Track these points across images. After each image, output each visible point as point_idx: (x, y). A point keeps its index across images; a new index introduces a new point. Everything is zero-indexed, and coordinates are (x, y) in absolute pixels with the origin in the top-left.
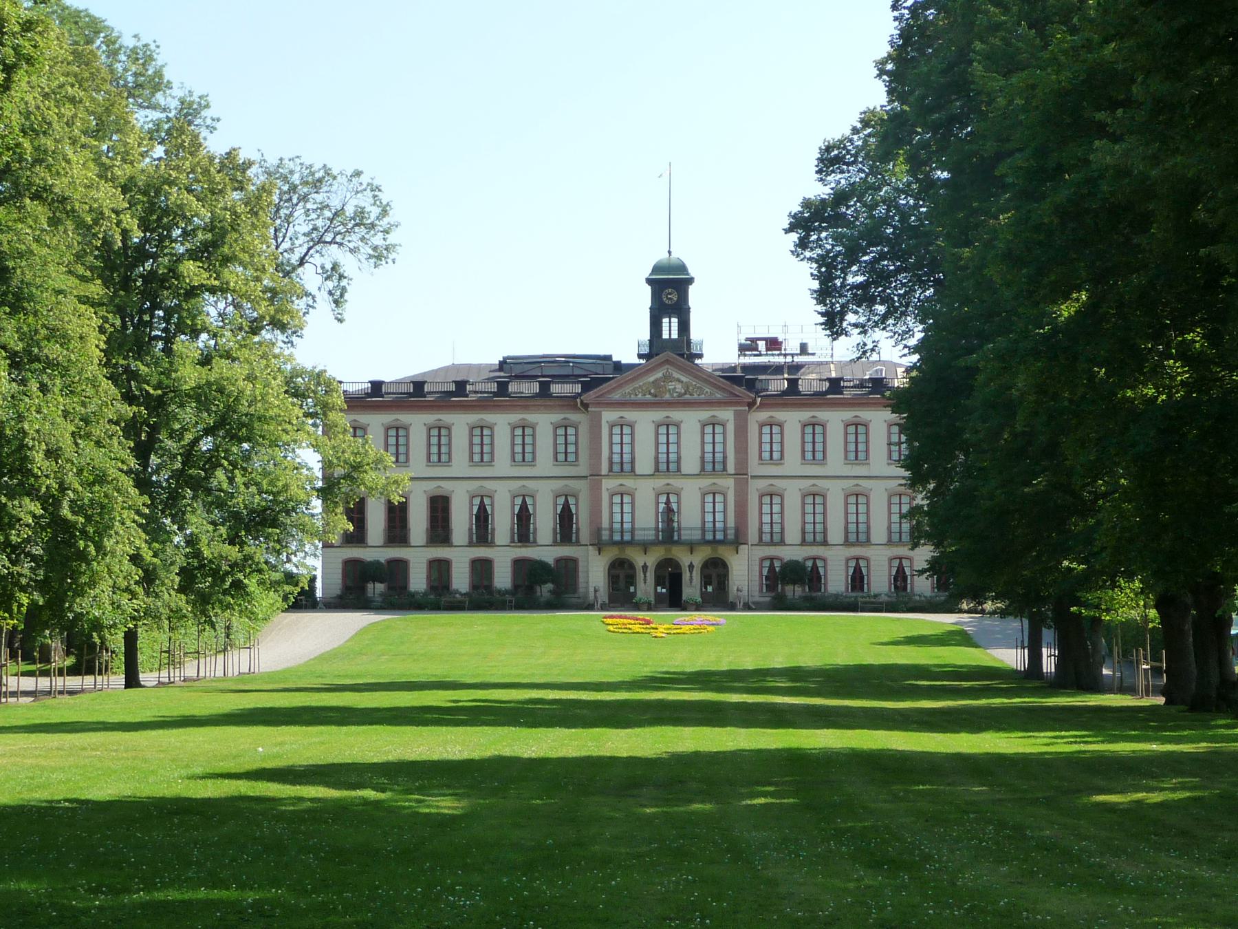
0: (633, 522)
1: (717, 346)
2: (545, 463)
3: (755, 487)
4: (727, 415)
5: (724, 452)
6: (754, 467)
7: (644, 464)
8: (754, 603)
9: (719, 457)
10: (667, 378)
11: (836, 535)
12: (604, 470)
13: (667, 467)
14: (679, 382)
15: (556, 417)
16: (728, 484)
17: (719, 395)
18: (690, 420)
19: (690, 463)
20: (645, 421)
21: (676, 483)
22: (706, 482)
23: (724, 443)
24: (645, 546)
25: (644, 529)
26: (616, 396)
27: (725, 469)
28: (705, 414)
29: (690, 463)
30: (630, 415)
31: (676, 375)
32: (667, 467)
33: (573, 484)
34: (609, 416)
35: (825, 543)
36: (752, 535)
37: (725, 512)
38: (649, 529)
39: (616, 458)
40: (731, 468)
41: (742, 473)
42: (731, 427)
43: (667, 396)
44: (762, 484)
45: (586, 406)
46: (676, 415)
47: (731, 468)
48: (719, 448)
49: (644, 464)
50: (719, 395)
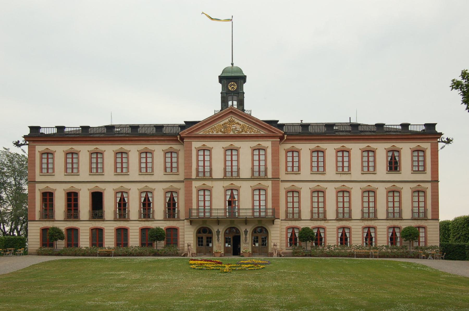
0: (211, 206)
1: (260, 104)
2: (159, 174)
3: (283, 187)
4: (267, 144)
5: (266, 165)
6: (283, 176)
7: (218, 173)
8: (283, 253)
9: (262, 169)
10: (231, 122)
11: (331, 214)
13: (231, 175)
14: (238, 126)
15: (166, 147)
16: (268, 184)
17: (262, 132)
18: (245, 147)
20: (218, 148)
21: (237, 183)
22: (254, 183)
23: (266, 160)
24: (218, 221)
26: (201, 133)
27: (266, 174)
28: (254, 144)
29: (245, 172)
30: (209, 144)
31: (236, 121)
32: (231, 175)
33: (176, 185)
35: (325, 219)
36: (282, 215)
37: (266, 200)
39: (201, 169)
40: (270, 175)
41: (276, 179)
42: (269, 151)
43: (232, 133)
44: (288, 185)
45: (182, 139)
46: (237, 144)
47: (270, 175)
48: (262, 163)
49: (218, 173)
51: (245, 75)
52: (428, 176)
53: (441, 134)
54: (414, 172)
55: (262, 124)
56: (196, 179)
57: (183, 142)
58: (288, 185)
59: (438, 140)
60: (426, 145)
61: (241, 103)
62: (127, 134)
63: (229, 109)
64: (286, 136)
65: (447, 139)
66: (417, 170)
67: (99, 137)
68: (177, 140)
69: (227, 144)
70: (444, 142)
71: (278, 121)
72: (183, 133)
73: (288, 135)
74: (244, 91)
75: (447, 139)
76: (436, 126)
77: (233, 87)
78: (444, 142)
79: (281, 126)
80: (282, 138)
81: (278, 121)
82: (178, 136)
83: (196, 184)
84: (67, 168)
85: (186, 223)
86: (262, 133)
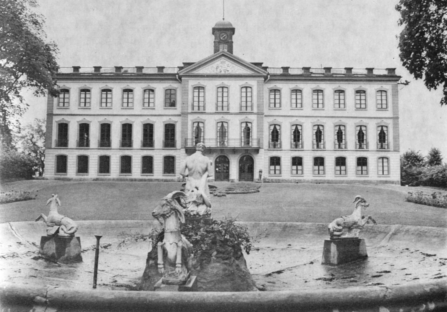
4: (253, 83)
12: (190, 110)
17: (249, 72)
18: (234, 85)
19: (234, 107)
20: (211, 85)
21: (227, 117)
25: (210, 139)
26: (196, 72)
29: (234, 107)
30: (202, 82)
34: (192, 83)
38: (212, 139)
39: (196, 104)
40: (255, 110)
41: (260, 114)
45: (180, 78)
46: (226, 82)
47: (255, 110)
50: (249, 72)
51: (234, 27)
52: (389, 113)
53: (400, 77)
54: (378, 109)
55: (249, 65)
56: (192, 113)
57: (181, 80)
58: (271, 120)
59: (398, 82)
60: (388, 86)
61: (231, 50)
62: (133, 73)
63: (221, 53)
64: (269, 76)
65: (406, 81)
66: (380, 107)
67: (110, 76)
68: (176, 80)
69: (218, 82)
70: (403, 84)
71: (262, 63)
72: (180, 73)
73: (272, 76)
74: (233, 40)
75: (406, 81)
76: (396, 71)
77: (224, 36)
78: (403, 84)
79: (266, 68)
80: (266, 78)
81: (262, 63)
82: (177, 76)
83: (191, 118)
84: (80, 102)
85: (183, 151)
86: (249, 73)
